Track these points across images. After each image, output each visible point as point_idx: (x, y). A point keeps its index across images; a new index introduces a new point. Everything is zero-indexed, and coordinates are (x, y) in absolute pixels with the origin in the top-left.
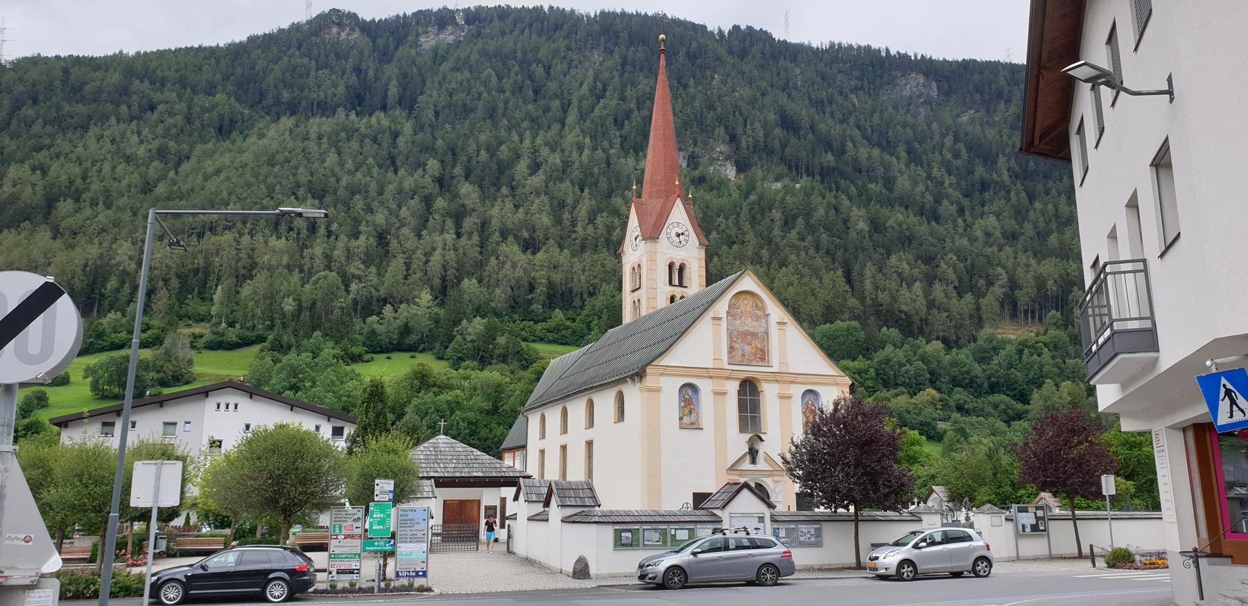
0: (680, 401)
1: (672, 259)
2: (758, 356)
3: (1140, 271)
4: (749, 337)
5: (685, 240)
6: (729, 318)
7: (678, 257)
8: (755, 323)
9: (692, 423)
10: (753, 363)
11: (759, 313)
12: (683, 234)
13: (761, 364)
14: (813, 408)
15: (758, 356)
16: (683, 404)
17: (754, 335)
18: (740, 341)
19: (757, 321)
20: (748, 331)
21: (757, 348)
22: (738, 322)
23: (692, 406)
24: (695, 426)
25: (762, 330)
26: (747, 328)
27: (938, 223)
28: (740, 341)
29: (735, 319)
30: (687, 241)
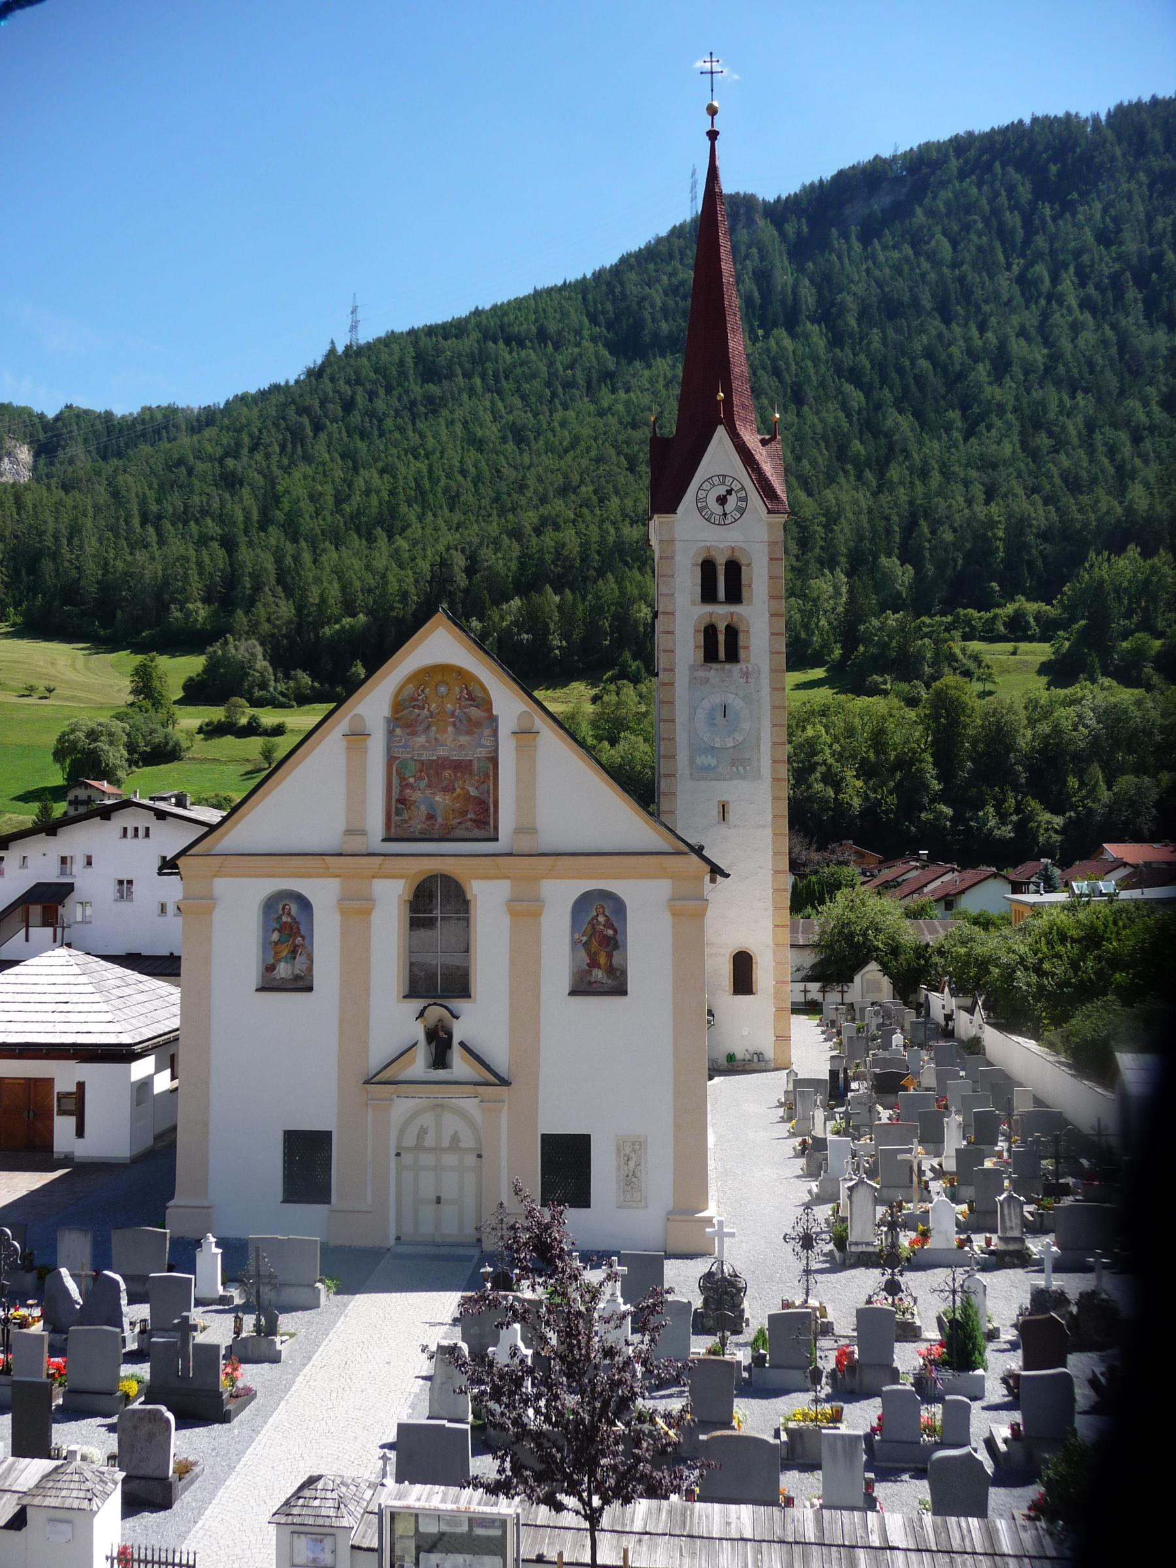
0: (266, 930)
1: (708, 549)
2: (471, 816)
3: (664, 721)
4: (447, 773)
5: (738, 509)
6: (398, 731)
7: (722, 546)
8: (464, 739)
9: (297, 978)
10: (458, 833)
11: (475, 713)
12: (729, 492)
13: (477, 833)
14: (610, 932)
15: (471, 816)
16: (275, 936)
17: (462, 767)
18: (423, 784)
19: (469, 733)
20: (446, 759)
21: (467, 797)
22: (421, 739)
23: (299, 940)
24: (301, 983)
25: (482, 752)
26: (442, 752)
27: (470, 397)
28: (423, 784)
29: (413, 734)
30: (742, 511)
